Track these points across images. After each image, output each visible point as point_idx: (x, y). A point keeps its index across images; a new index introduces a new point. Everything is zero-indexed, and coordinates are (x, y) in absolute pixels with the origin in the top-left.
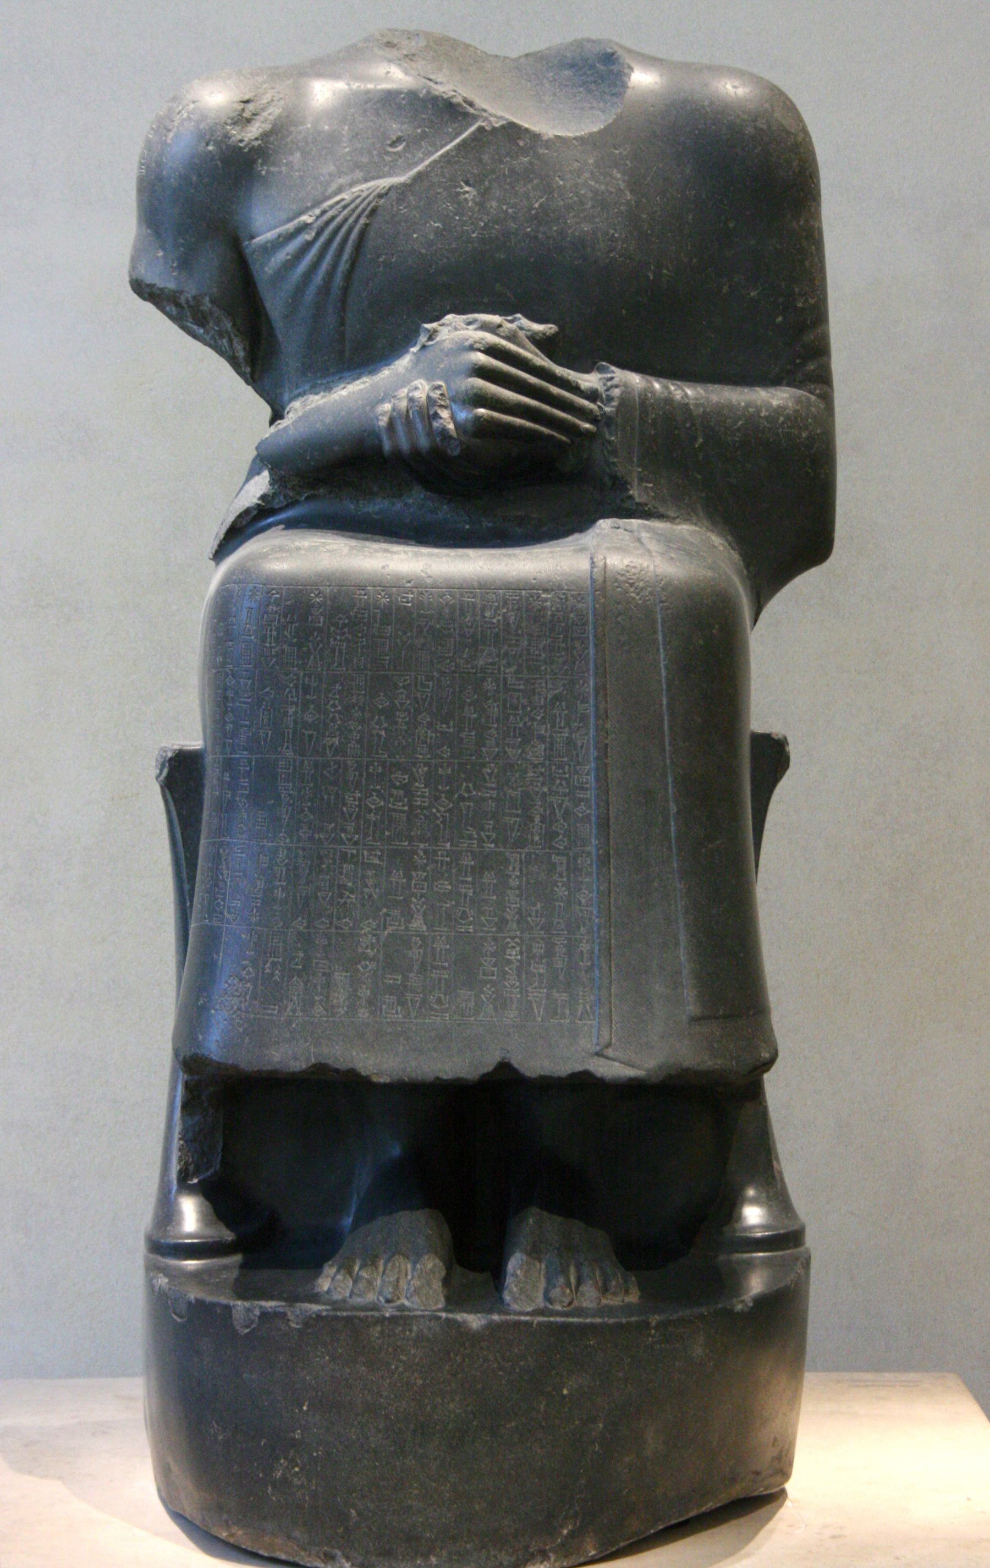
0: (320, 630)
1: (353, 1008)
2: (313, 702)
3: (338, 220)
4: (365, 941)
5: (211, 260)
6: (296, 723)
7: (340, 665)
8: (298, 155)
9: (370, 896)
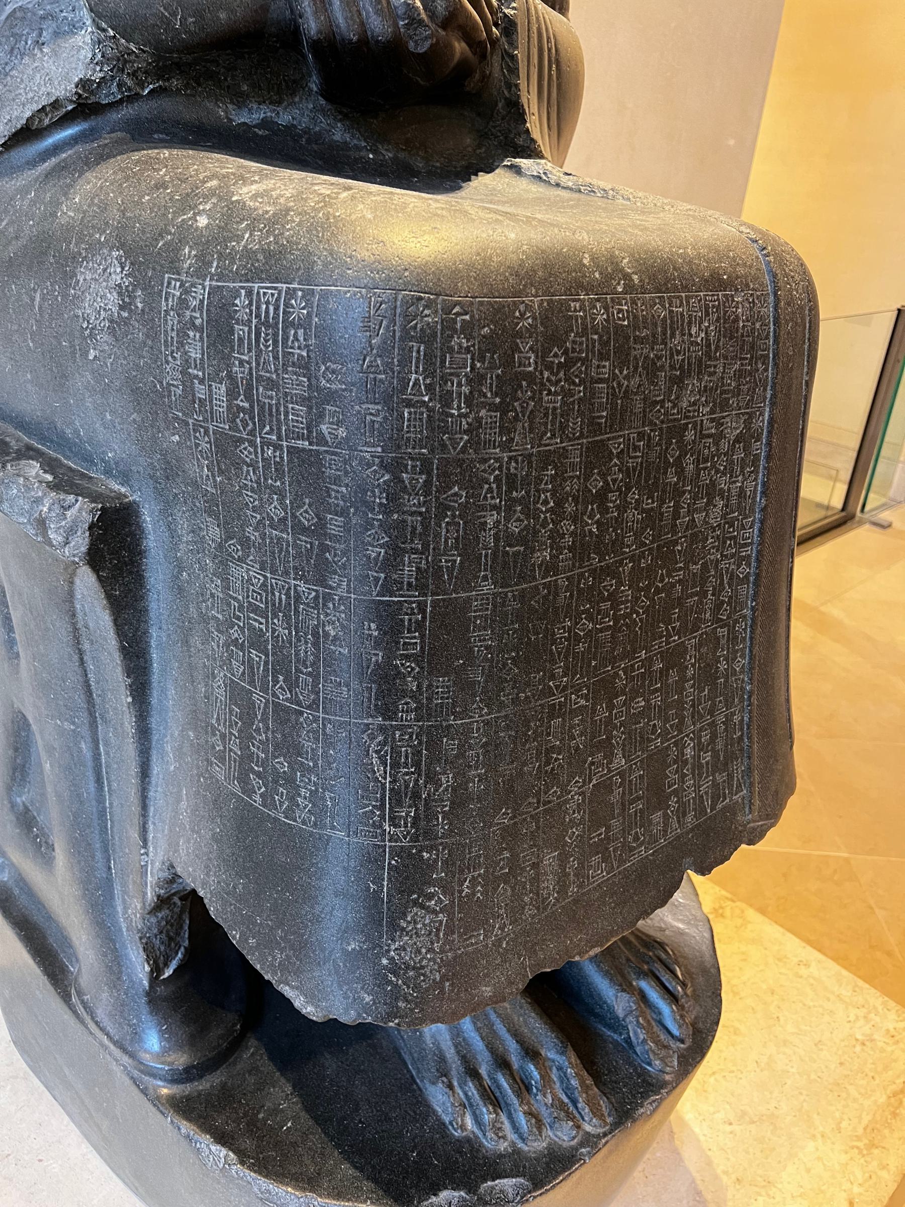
6: (497, 538)
7: (553, 436)
9: (577, 748)
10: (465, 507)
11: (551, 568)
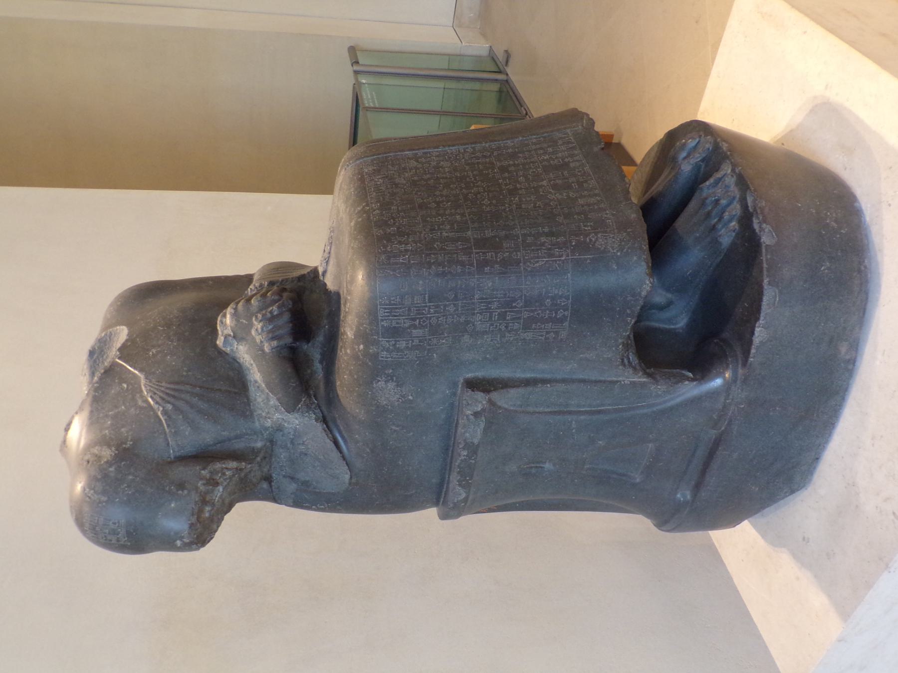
0: (398, 228)
1: (596, 195)
2: (439, 226)
3: (161, 394)
4: (560, 197)
5: (181, 472)
8: (123, 430)
10: (441, 243)
11: (463, 215)
